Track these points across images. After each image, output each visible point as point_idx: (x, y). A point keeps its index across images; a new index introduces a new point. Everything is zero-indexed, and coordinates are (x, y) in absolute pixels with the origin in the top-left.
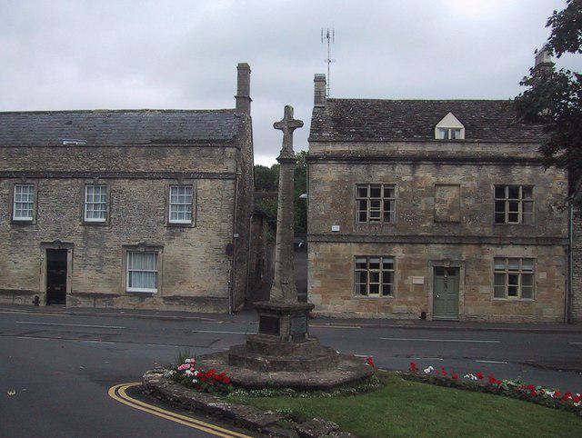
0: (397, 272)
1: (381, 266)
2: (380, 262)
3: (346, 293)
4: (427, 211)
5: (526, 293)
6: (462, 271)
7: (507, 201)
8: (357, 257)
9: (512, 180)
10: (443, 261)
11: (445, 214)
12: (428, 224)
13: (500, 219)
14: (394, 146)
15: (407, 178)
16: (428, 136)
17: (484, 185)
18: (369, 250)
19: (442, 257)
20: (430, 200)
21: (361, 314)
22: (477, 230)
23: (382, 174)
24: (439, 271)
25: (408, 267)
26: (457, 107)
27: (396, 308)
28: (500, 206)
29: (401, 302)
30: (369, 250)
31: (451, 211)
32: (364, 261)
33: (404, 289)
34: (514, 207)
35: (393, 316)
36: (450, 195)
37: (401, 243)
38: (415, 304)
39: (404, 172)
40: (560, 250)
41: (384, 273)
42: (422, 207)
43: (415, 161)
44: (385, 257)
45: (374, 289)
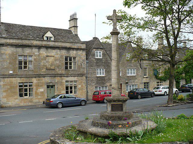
0: (34, 88)
1: (28, 86)
2: (28, 84)
3: (16, 97)
4: (44, 65)
5: (75, 93)
6: (56, 86)
7: (68, 62)
8: (19, 83)
9: (70, 55)
10: (50, 83)
11: (49, 66)
12: (44, 70)
13: (66, 68)
14: (32, 42)
15: (37, 53)
16: (42, 39)
17: (62, 56)
18: (24, 80)
19: (49, 82)
20: (45, 61)
21: (22, 104)
22: (60, 72)
23: (28, 52)
24: (48, 87)
25: (38, 86)
26: (53, 30)
27: (35, 101)
28: (66, 63)
29: (36, 99)
30: (24, 80)
31: (51, 66)
32: (22, 84)
33: (37, 94)
34: (70, 64)
35: (34, 104)
36: (51, 60)
37: (35, 77)
38: (41, 99)
39: (35, 51)
40: (84, 77)
41: (29, 89)
42: (42, 64)
43: (39, 47)
44: (29, 82)
45: (26, 95)
